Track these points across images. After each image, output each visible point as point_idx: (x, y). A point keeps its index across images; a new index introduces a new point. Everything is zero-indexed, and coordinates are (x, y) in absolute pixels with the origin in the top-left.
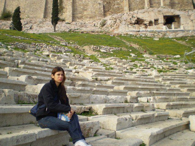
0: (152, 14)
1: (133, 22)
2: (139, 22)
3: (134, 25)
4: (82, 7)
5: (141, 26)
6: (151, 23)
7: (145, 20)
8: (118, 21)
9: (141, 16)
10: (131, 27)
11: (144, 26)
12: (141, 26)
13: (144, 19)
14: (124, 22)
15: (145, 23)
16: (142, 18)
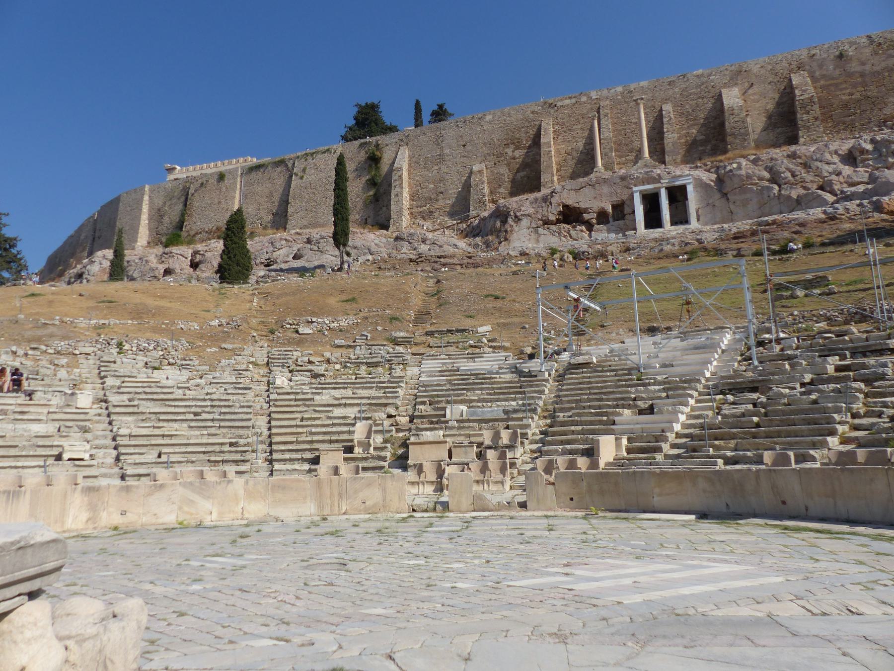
0: (605, 189)
1: (553, 218)
2: (571, 216)
3: (553, 227)
4: (432, 186)
5: (574, 227)
6: (603, 217)
7: (586, 210)
8: (510, 220)
9: (571, 199)
10: (546, 232)
11: (584, 228)
12: (574, 227)
13: (583, 205)
14: (525, 222)
15: (586, 216)
16: (576, 205)
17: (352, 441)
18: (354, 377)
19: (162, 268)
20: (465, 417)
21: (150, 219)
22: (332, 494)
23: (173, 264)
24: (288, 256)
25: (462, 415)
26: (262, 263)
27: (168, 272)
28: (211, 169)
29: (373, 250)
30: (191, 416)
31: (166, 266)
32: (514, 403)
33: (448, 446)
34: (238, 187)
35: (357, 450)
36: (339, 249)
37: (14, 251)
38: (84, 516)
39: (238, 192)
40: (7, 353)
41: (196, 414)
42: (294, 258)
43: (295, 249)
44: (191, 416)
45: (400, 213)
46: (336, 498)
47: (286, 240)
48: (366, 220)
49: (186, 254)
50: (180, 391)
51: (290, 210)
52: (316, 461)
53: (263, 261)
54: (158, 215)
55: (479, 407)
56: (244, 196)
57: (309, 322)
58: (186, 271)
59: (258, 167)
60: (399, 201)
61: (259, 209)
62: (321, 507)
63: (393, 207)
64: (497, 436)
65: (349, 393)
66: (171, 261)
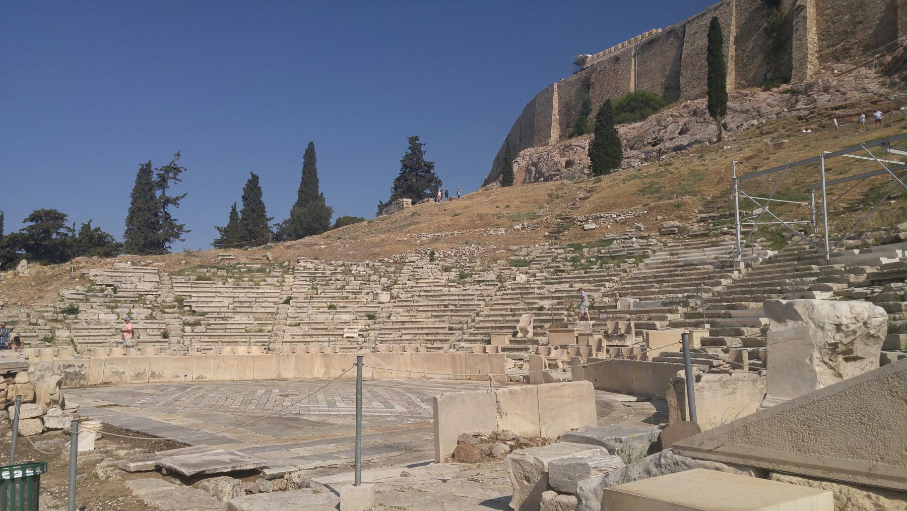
17: (515, 327)
18: (583, 271)
19: (563, 161)
20: (632, 308)
21: (560, 114)
22: (461, 366)
23: (571, 155)
24: (674, 132)
25: (629, 307)
26: (649, 143)
27: (569, 164)
28: (614, 50)
29: (763, 111)
30: (443, 308)
31: (566, 159)
32: (680, 295)
33: (576, 334)
34: (633, 67)
35: (520, 335)
36: (715, 118)
37: (432, 171)
38: (322, 371)
39: (633, 73)
40: (363, 265)
41: (445, 306)
42: (680, 134)
43: (681, 123)
44: (443, 308)
45: (804, 60)
46: (464, 368)
47: (672, 116)
48: (765, 75)
49: (583, 145)
50: (447, 289)
51: (683, 81)
52: (489, 342)
53: (649, 141)
54: (566, 109)
55: (651, 299)
56: (638, 76)
57: (598, 218)
58: (584, 161)
59: (651, 42)
60: (803, 47)
61: (653, 86)
62: (455, 372)
63: (795, 54)
64: (617, 328)
65: (566, 286)
66: (571, 153)
